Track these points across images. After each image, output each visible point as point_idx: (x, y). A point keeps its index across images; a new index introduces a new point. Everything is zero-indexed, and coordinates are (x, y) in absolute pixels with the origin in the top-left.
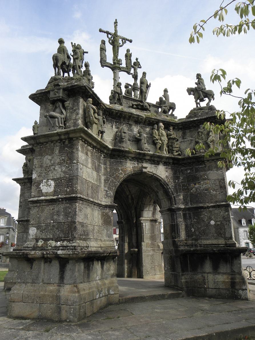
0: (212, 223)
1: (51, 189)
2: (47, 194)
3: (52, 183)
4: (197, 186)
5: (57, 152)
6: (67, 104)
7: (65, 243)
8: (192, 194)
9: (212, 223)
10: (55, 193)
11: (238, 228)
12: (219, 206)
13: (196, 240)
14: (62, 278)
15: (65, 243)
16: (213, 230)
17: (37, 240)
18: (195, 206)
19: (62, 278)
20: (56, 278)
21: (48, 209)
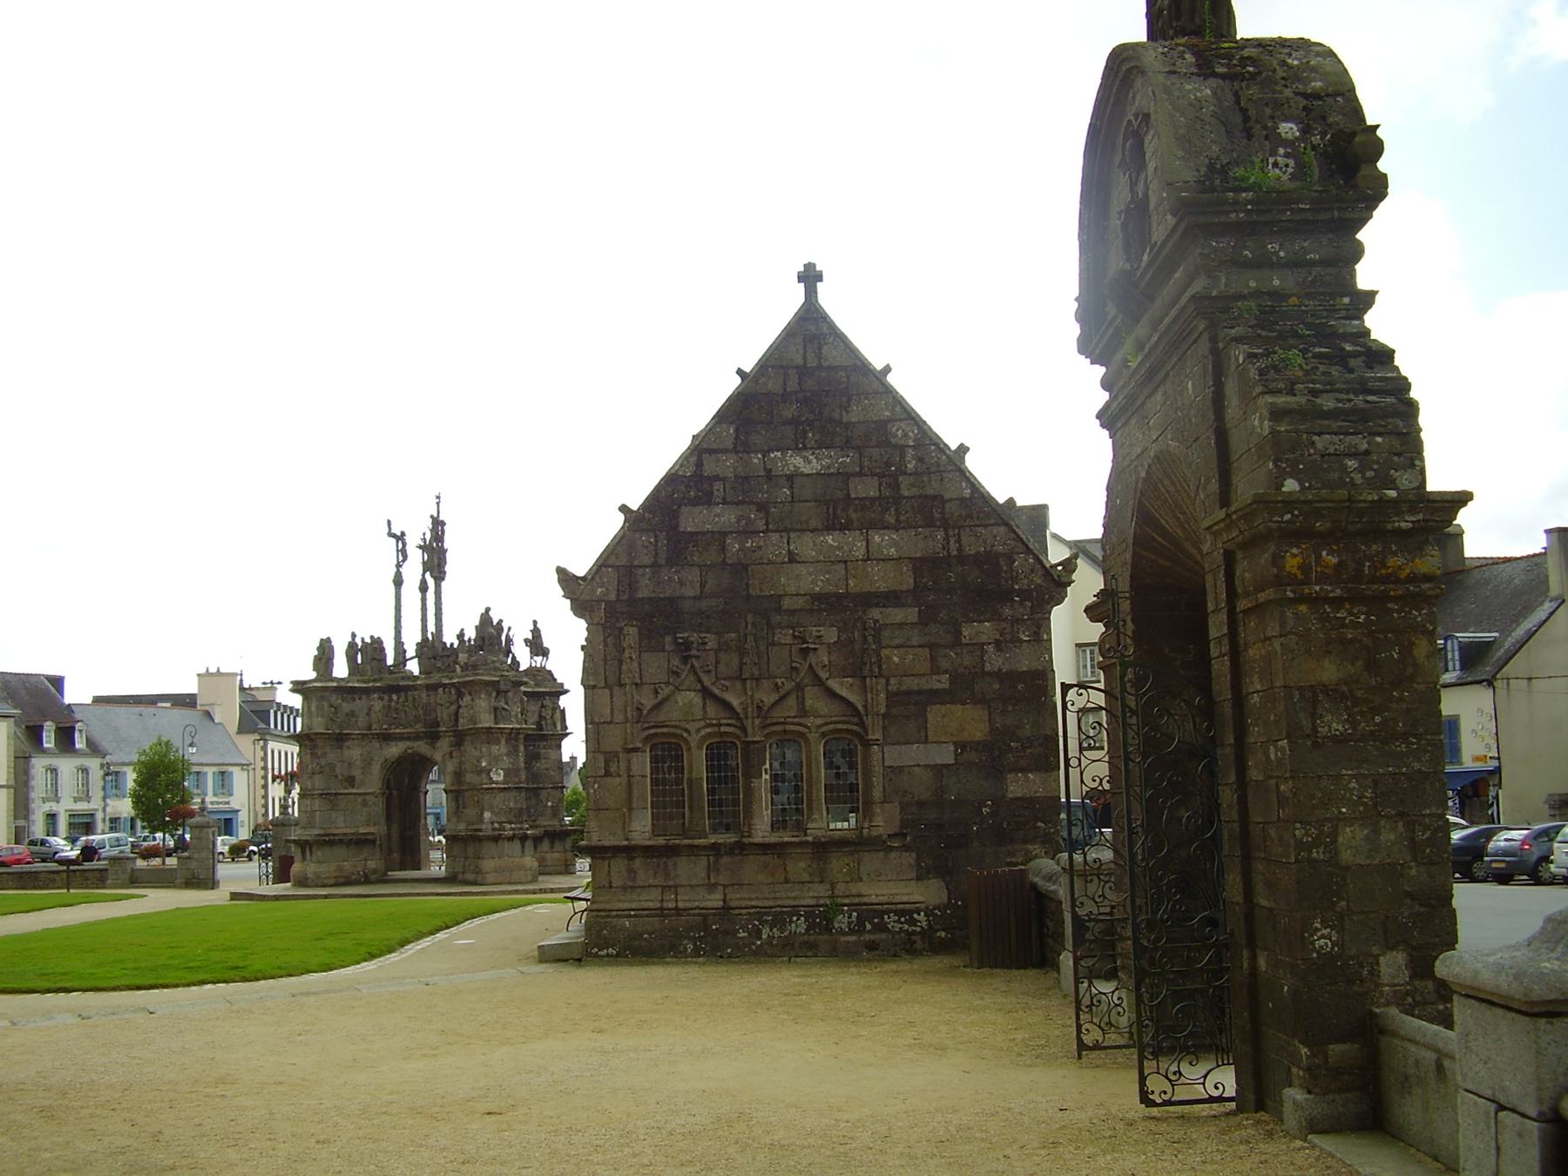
0: (550, 804)
1: (501, 778)
2: (497, 783)
3: (502, 772)
4: (538, 764)
5: (504, 743)
6: (510, 694)
7: (518, 826)
8: (533, 774)
9: (550, 804)
10: (504, 782)
11: (27, 758)
12: (557, 788)
13: (534, 821)
14: (523, 852)
15: (518, 826)
16: (549, 811)
17: (492, 823)
18: (535, 786)
19: (523, 852)
20: (520, 854)
21: (500, 797)
